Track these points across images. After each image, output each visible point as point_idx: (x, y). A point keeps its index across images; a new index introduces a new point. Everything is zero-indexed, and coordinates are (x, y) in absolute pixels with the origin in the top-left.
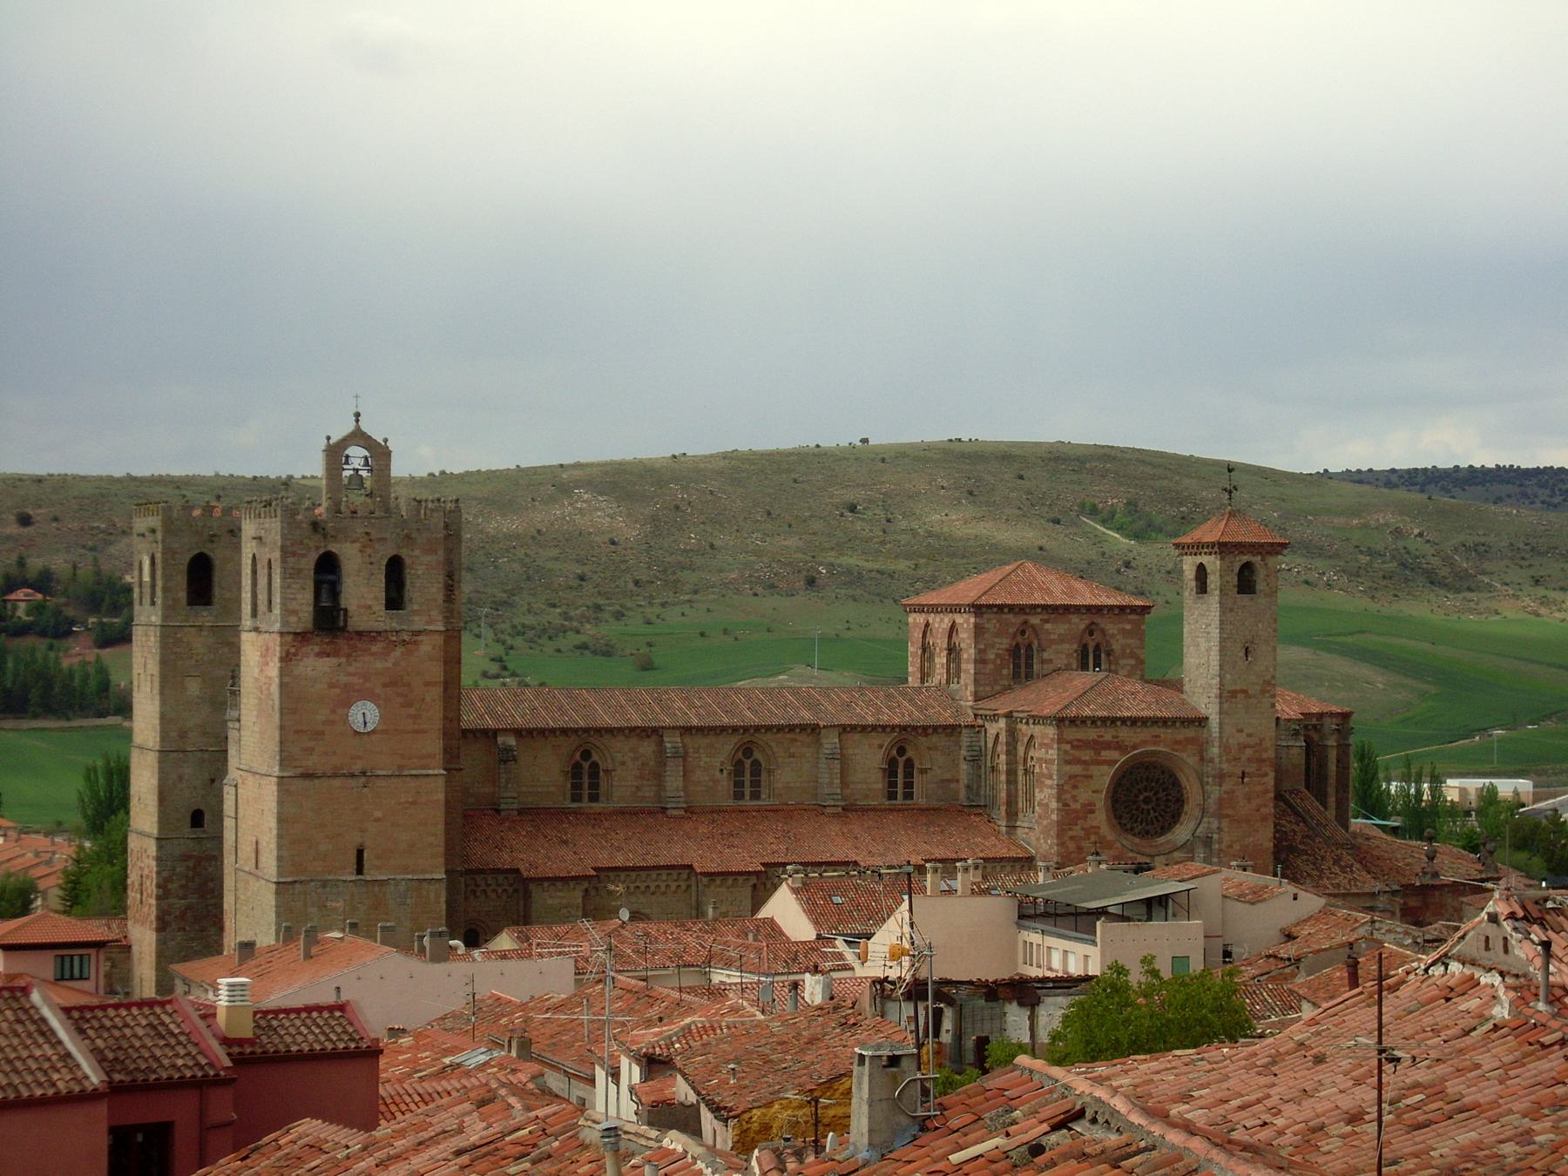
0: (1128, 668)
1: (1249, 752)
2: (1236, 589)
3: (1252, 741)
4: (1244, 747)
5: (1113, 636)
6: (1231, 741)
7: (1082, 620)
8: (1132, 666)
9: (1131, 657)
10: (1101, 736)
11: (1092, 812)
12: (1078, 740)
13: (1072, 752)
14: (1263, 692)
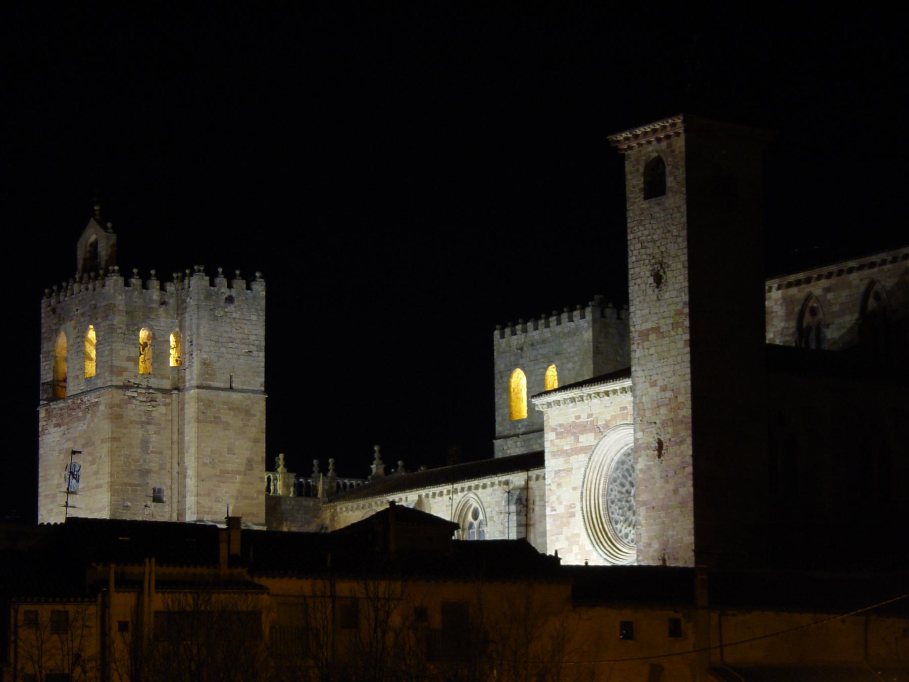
2: (642, 196)
6: (644, 400)
10: (578, 417)
11: (573, 515)
12: (561, 425)
13: (556, 441)
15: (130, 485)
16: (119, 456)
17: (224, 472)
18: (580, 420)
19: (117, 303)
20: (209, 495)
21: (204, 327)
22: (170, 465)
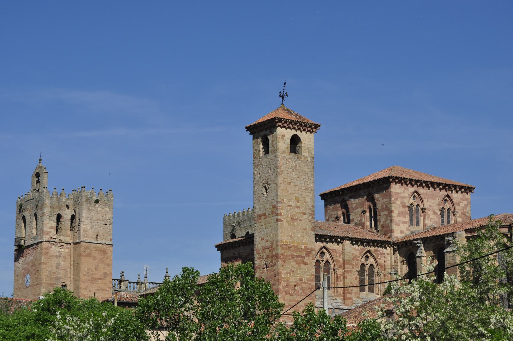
0: (385, 217)
1: (267, 251)
3: (268, 244)
4: (264, 249)
5: (378, 198)
7: (365, 193)
8: (386, 215)
9: (385, 210)
10: (234, 254)
14: (273, 212)
15: (51, 284)
16: (46, 271)
17: (93, 279)
18: (235, 255)
19: (46, 202)
20: (86, 289)
21: (85, 214)
22: (69, 275)
